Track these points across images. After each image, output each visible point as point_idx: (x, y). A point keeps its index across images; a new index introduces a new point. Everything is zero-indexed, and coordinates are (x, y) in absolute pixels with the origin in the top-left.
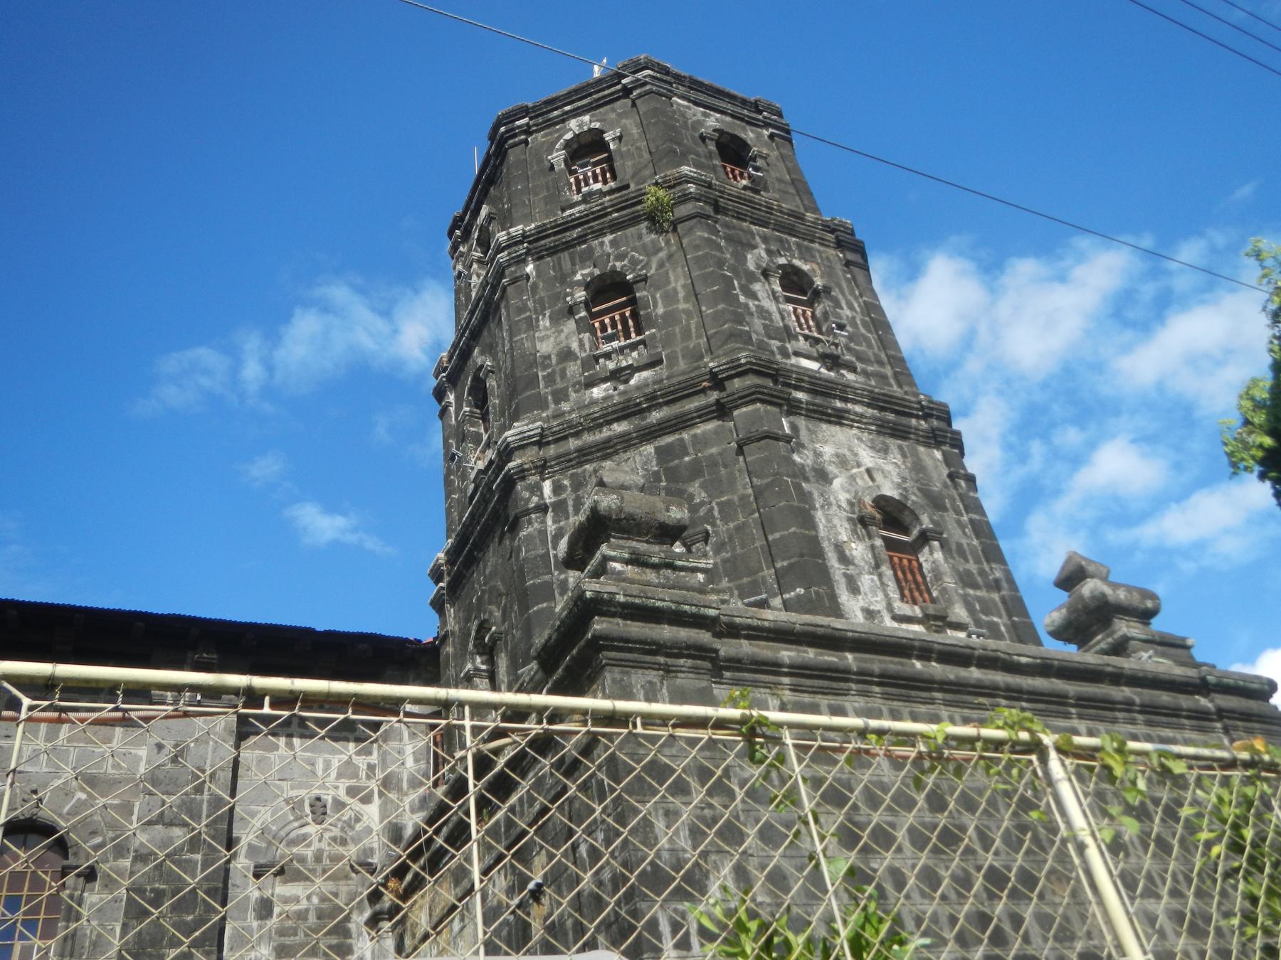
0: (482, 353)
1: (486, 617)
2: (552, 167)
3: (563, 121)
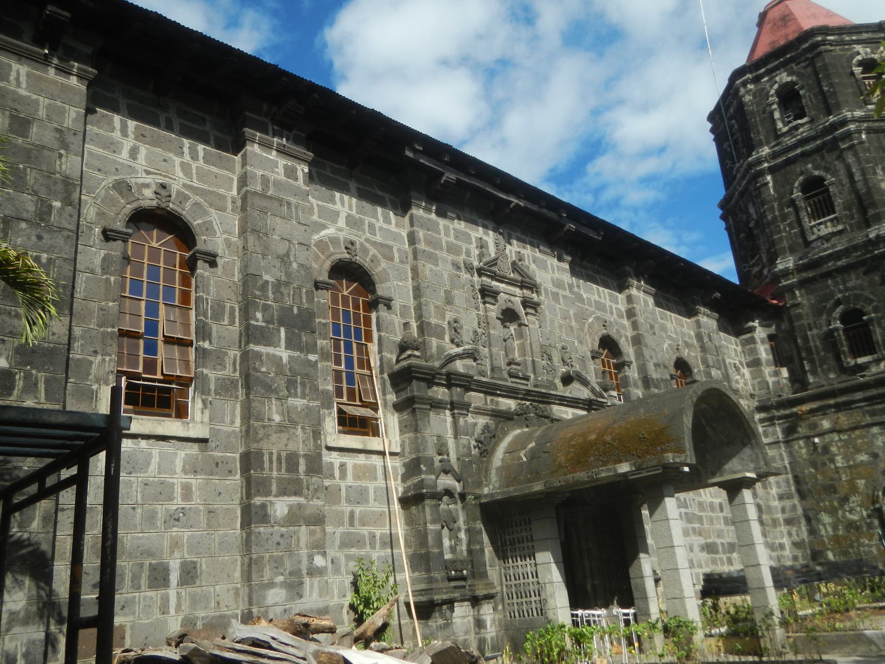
0: (816, 168)
1: (858, 307)
2: (852, 74)
3: (850, 44)
